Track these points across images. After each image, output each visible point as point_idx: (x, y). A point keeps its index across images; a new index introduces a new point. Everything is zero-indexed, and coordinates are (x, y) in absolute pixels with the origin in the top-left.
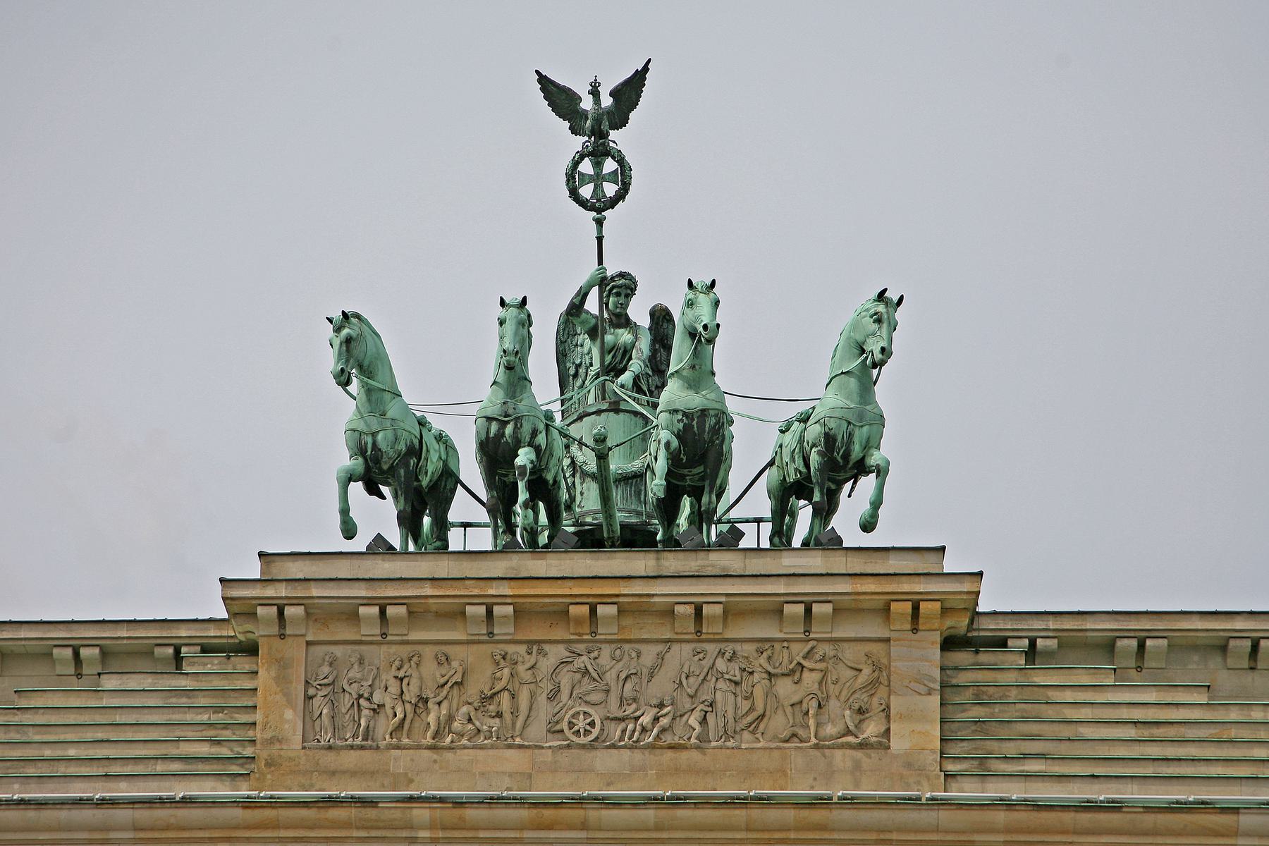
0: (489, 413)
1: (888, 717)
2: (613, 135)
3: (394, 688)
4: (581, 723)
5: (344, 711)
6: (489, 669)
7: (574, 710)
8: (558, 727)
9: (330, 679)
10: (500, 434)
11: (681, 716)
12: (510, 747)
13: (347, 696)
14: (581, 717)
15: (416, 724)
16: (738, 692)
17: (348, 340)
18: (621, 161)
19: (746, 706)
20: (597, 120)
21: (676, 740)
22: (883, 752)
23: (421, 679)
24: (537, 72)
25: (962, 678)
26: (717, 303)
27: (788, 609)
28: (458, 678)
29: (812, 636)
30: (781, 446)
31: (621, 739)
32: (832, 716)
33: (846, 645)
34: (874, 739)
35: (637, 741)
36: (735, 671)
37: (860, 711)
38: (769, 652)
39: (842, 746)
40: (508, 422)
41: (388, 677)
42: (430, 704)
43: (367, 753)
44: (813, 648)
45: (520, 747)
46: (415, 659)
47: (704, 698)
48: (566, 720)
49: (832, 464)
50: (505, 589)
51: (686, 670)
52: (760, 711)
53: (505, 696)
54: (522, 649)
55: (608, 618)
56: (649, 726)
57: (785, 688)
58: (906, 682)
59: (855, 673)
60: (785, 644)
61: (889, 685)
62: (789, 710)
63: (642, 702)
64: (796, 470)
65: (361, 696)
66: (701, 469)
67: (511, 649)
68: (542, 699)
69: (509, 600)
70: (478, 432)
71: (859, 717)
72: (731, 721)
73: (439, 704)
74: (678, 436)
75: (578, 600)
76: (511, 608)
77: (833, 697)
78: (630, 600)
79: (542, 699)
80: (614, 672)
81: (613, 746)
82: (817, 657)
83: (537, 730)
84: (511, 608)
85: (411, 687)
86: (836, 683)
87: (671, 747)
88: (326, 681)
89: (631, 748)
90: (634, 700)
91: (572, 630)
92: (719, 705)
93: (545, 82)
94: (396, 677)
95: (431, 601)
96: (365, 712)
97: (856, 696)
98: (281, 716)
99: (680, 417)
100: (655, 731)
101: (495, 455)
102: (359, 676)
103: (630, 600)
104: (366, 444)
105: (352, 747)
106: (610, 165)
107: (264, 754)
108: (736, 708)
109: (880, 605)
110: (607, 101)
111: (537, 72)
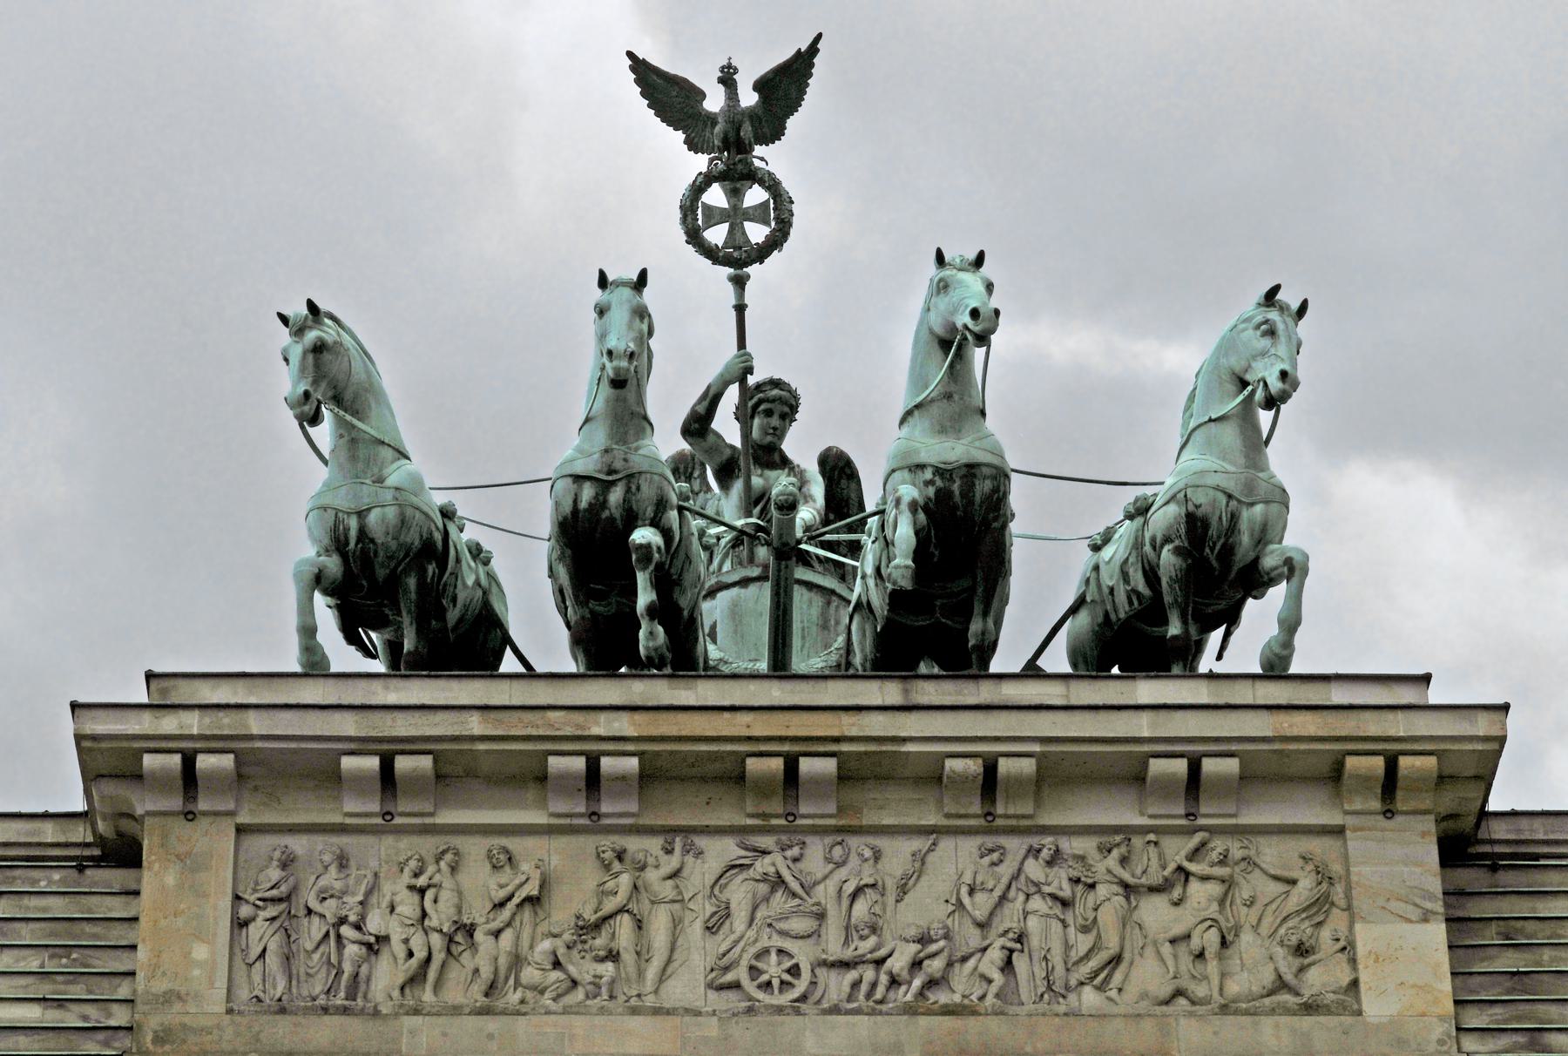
0: (580, 468)
1: (1353, 961)
2: (759, 150)
3: (408, 906)
4: (773, 969)
5: (309, 946)
6: (591, 876)
7: (759, 946)
8: (729, 977)
9: (284, 889)
10: (599, 504)
11: (964, 959)
12: (634, 1011)
13: (316, 920)
14: (774, 957)
15: (456, 974)
16: (1070, 920)
17: (319, 348)
18: (773, 186)
19: (1083, 943)
20: (734, 131)
21: (957, 998)
22: (1348, 1020)
23: (460, 893)
24: (630, 55)
25: (1476, 909)
26: (989, 287)
27: (1156, 766)
28: (532, 889)
29: (1202, 821)
30: (1096, 568)
31: (850, 999)
32: (1248, 962)
33: (1262, 841)
34: (1331, 996)
35: (881, 1002)
36: (1059, 881)
37: (1301, 950)
38: (1123, 849)
39: (1272, 1011)
40: (613, 483)
41: (396, 887)
42: (479, 936)
43: (354, 1025)
44: (1203, 844)
45: (657, 1011)
46: (449, 857)
47: (1007, 925)
48: (744, 963)
49: (1208, 569)
50: (623, 725)
51: (968, 879)
52: (1117, 950)
53: (624, 924)
54: (654, 844)
55: (818, 781)
56: (905, 974)
57: (1156, 913)
58: (1381, 902)
59: (1281, 887)
60: (1152, 837)
61: (1349, 908)
62: (1167, 949)
63: (887, 934)
64: (1133, 593)
65: (342, 921)
66: (965, 583)
67: (633, 844)
68: (694, 931)
69: (630, 747)
70: (557, 504)
71: (1297, 962)
72: (1060, 970)
73: (497, 934)
74: (926, 509)
75: (763, 748)
76: (634, 762)
77: (1247, 927)
78: (861, 748)
79: (694, 931)
80: (831, 886)
81: (835, 1010)
82: (1214, 856)
83: (686, 987)
84: (634, 762)
85: (441, 904)
86: (1250, 903)
87: (948, 1011)
88: (274, 892)
89: (873, 1012)
90: (874, 929)
91: (750, 810)
92: (1035, 941)
93: (643, 71)
94: (411, 888)
95: (482, 747)
96: (352, 950)
97: (1290, 923)
98: (187, 955)
99: (928, 475)
100: (917, 983)
101: (592, 547)
102: (338, 885)
103: (861, 748)
104: (347, 530)
105: (325, 1010)
106: (755, 195)
107: (153, 1023)
108: (1067, 947)
109: (1325, 767)
110: (748, 98)
111: (630, 55)
